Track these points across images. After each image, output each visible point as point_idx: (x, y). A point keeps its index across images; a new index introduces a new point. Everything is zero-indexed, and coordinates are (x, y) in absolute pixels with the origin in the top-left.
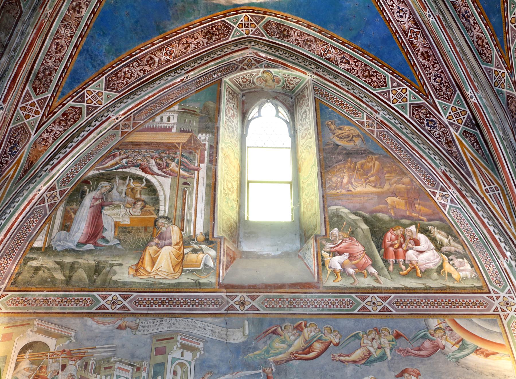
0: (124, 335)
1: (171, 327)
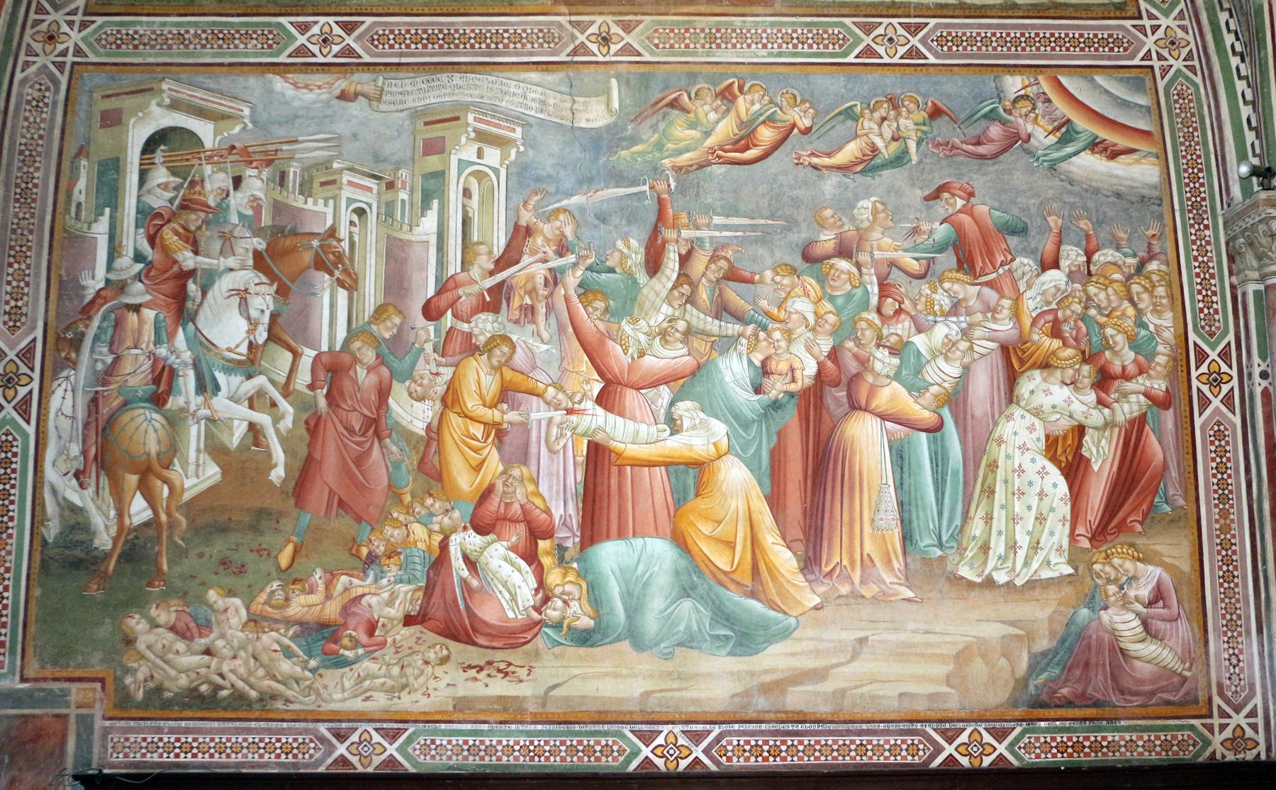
0: (355, 113)
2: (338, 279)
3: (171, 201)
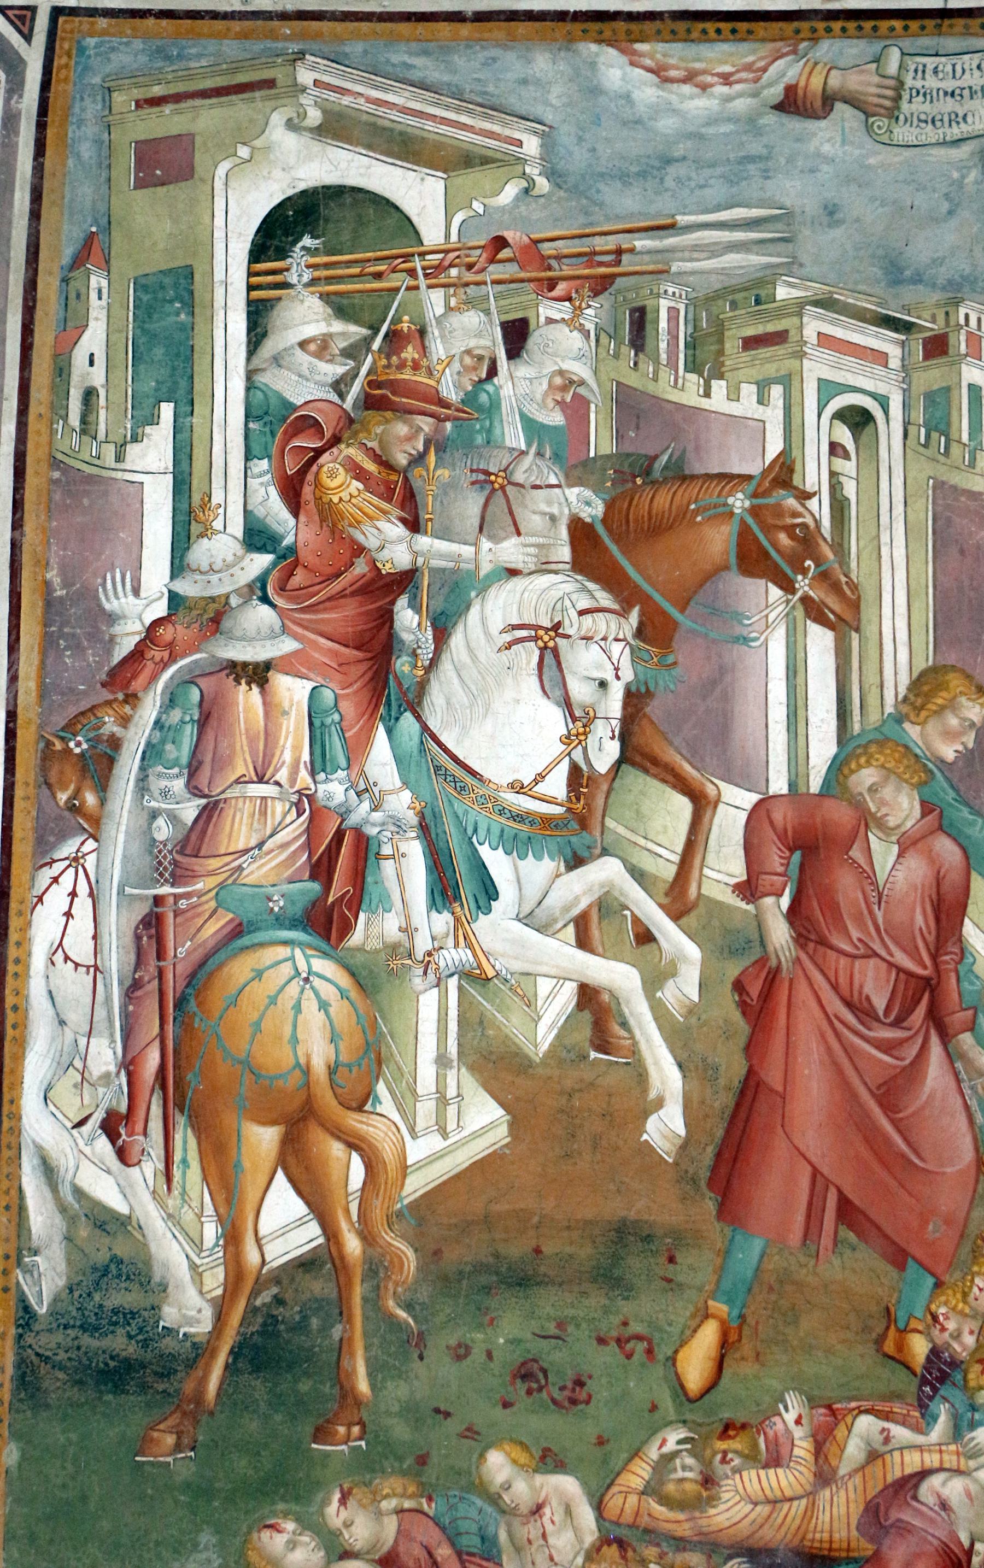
0: (826, 148)
2: (805, 600)
3: (340, 386)
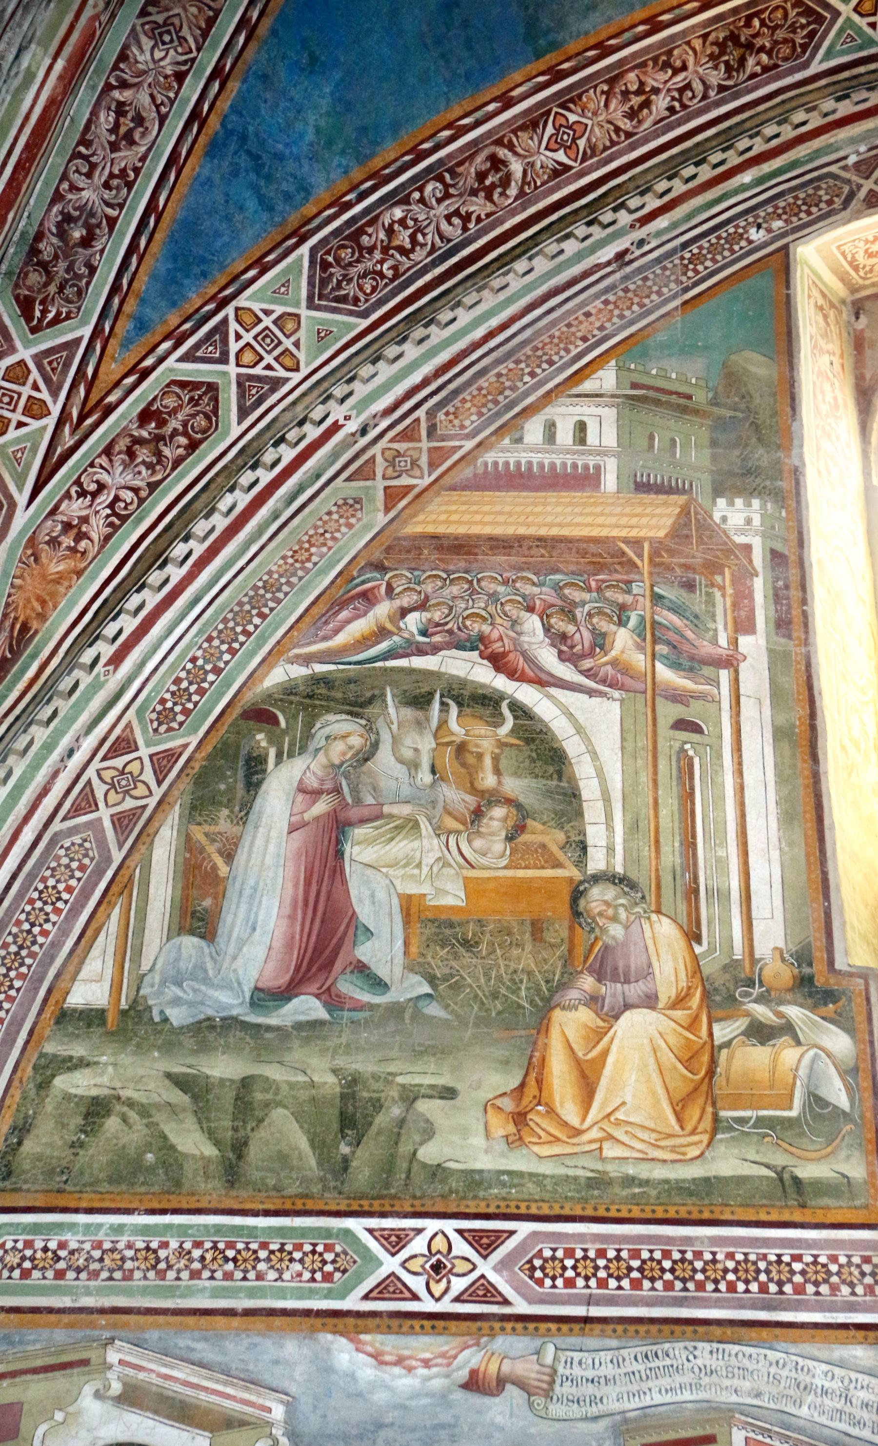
0: (499, 1419)
1: (699, 1386)
